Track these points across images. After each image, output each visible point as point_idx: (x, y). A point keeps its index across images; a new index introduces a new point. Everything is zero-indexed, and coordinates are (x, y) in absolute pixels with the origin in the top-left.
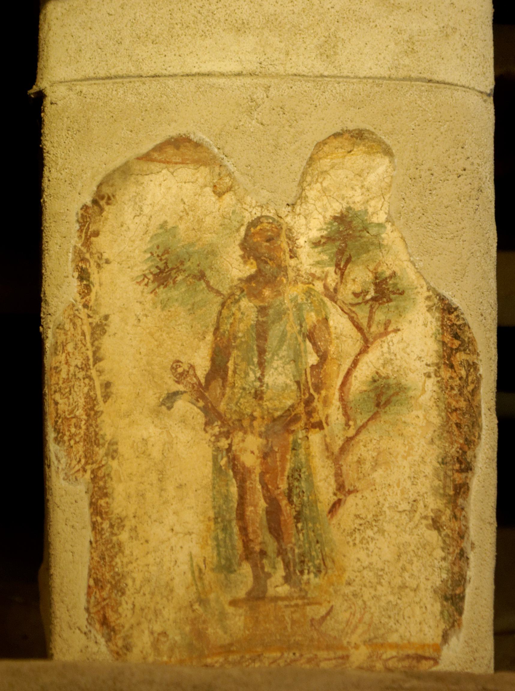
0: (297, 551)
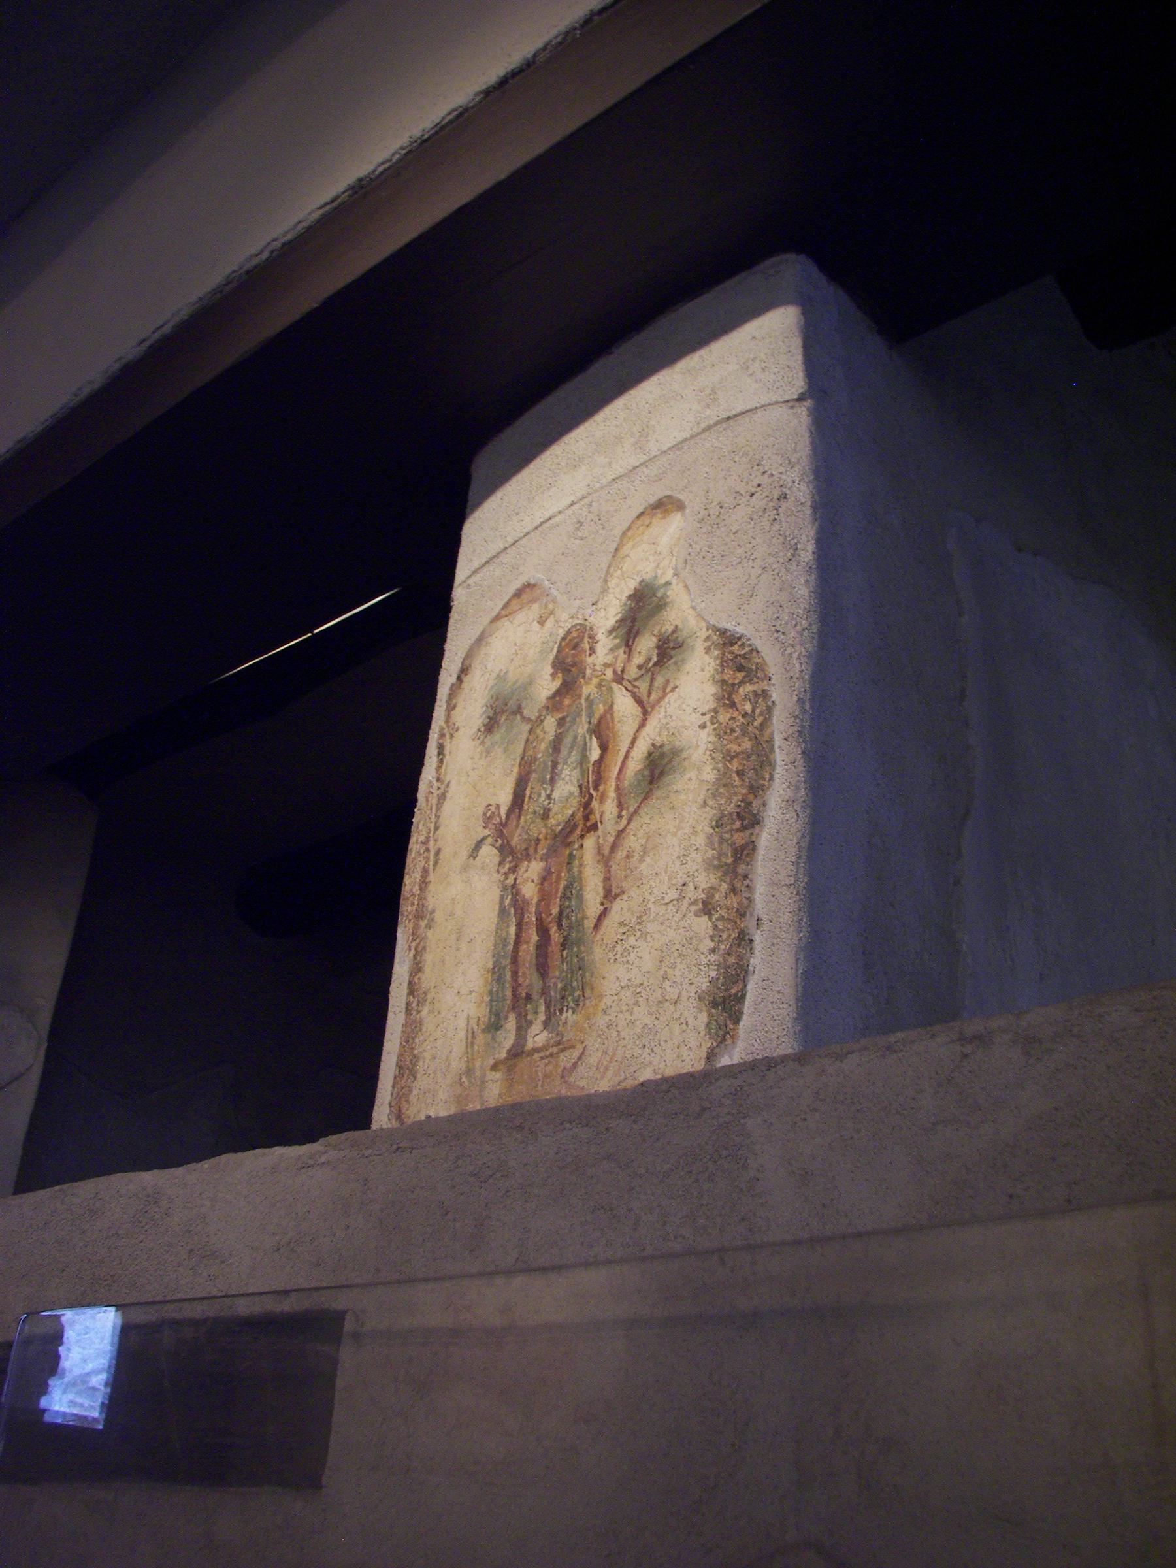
0: (559, 985)
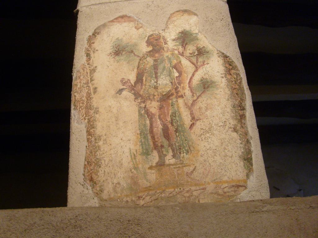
0: (177, 144)
